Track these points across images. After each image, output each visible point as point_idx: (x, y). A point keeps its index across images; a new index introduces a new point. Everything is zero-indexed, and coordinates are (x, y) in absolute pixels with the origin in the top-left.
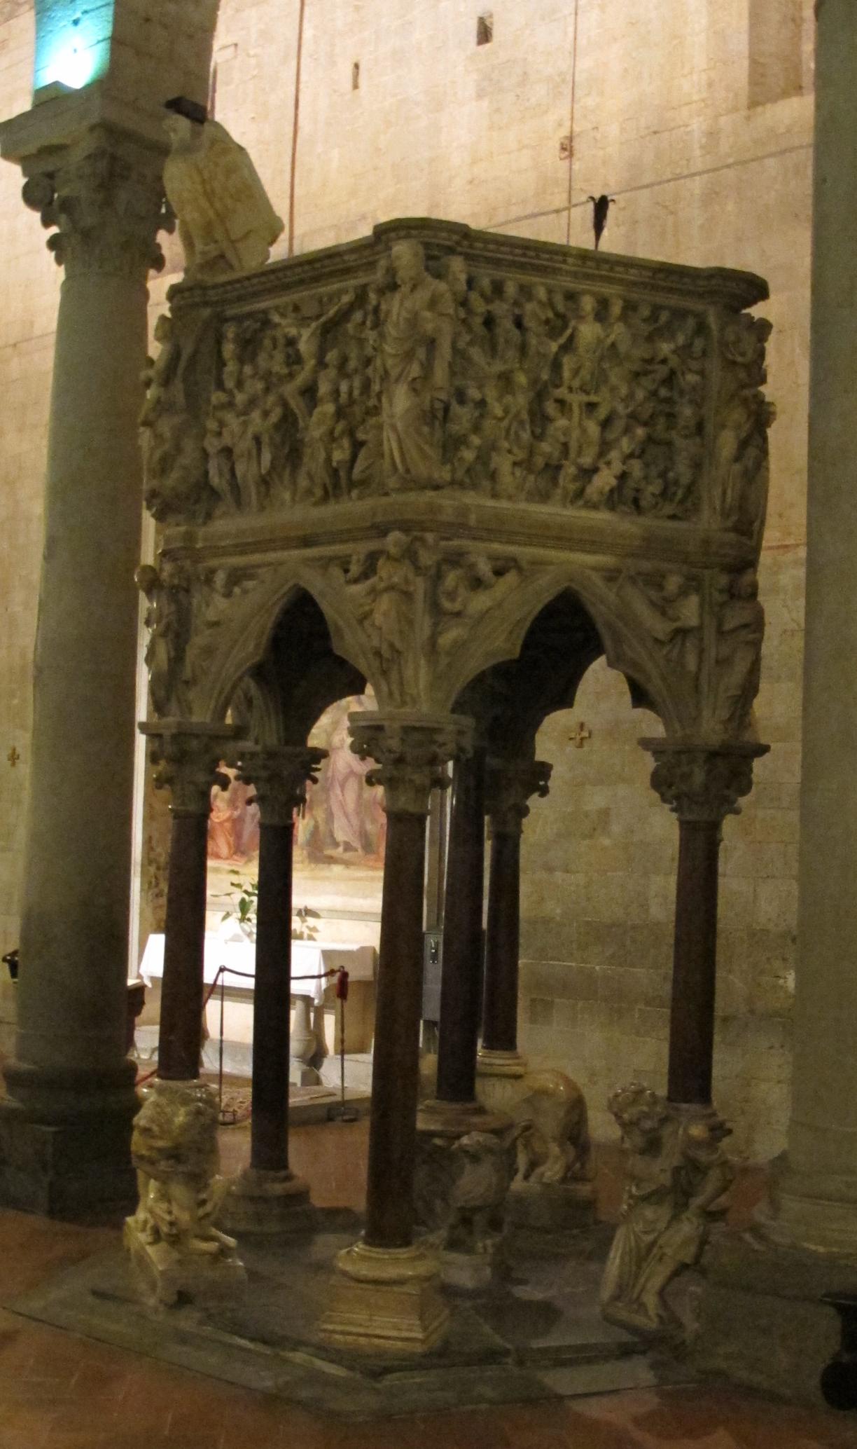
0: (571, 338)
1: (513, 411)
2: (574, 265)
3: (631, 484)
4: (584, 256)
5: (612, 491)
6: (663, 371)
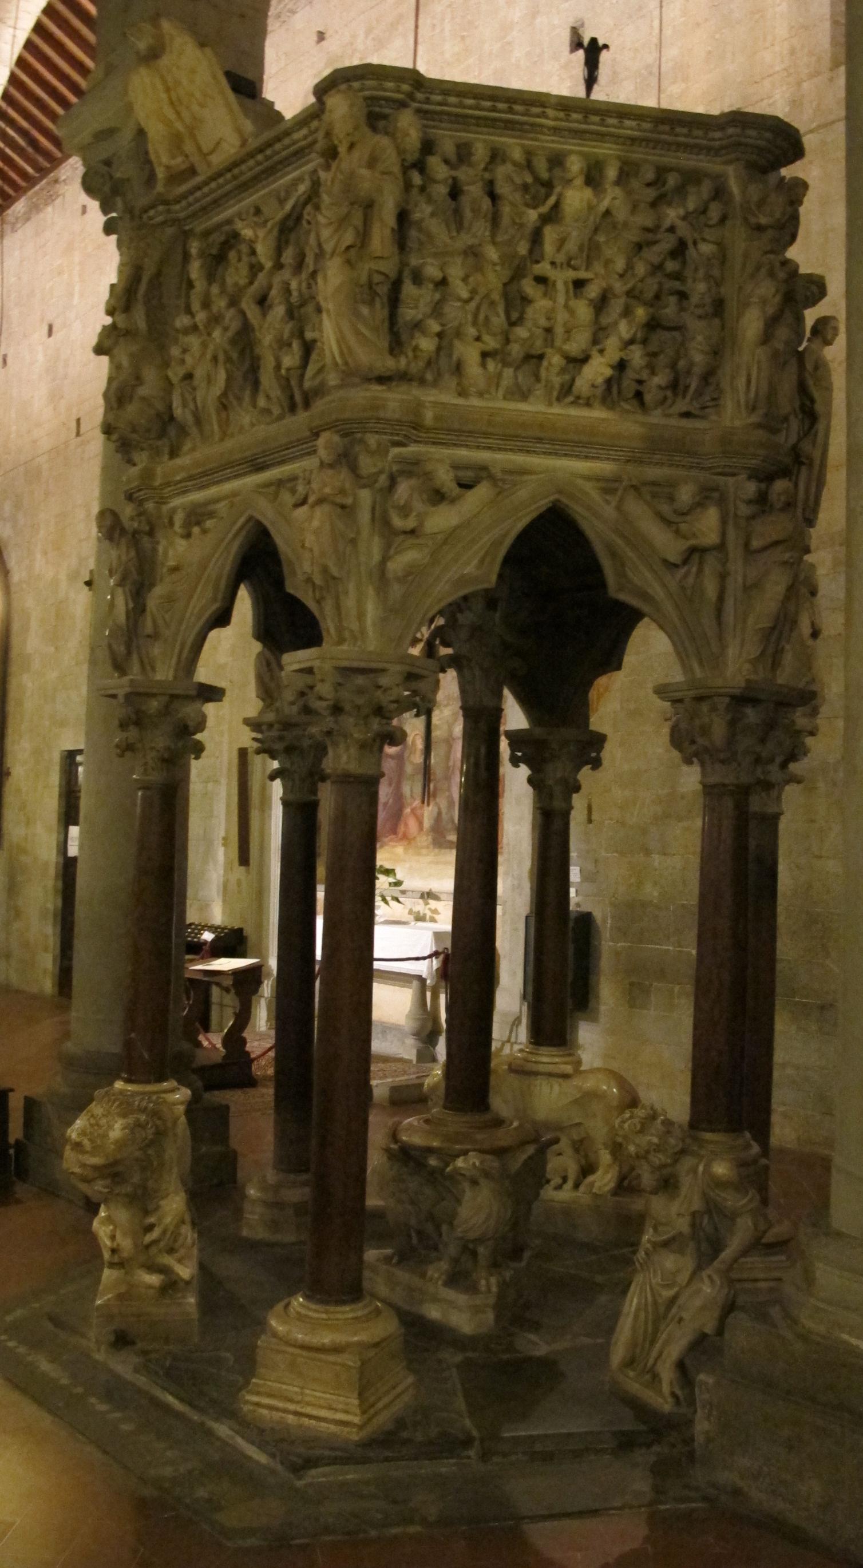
0: (556, 206)
1: (482, 291)
2: (556, 119)
3: (630, 374)
4: (565, 105)
5: (609, 382)
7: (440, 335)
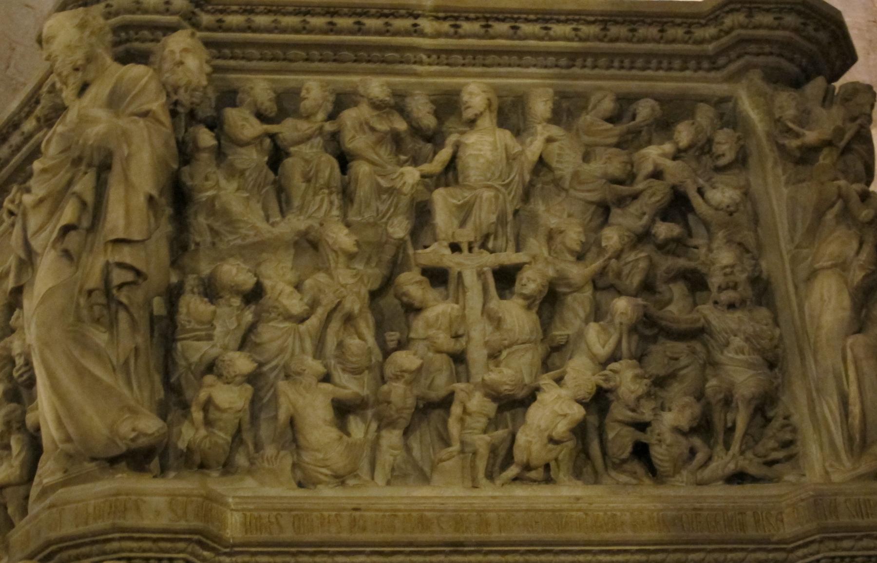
1: (328, 301)
2: (438, 35)
3: (618, 412)
5: (580, 430)
6: (655, 195)
7: (253, 378)
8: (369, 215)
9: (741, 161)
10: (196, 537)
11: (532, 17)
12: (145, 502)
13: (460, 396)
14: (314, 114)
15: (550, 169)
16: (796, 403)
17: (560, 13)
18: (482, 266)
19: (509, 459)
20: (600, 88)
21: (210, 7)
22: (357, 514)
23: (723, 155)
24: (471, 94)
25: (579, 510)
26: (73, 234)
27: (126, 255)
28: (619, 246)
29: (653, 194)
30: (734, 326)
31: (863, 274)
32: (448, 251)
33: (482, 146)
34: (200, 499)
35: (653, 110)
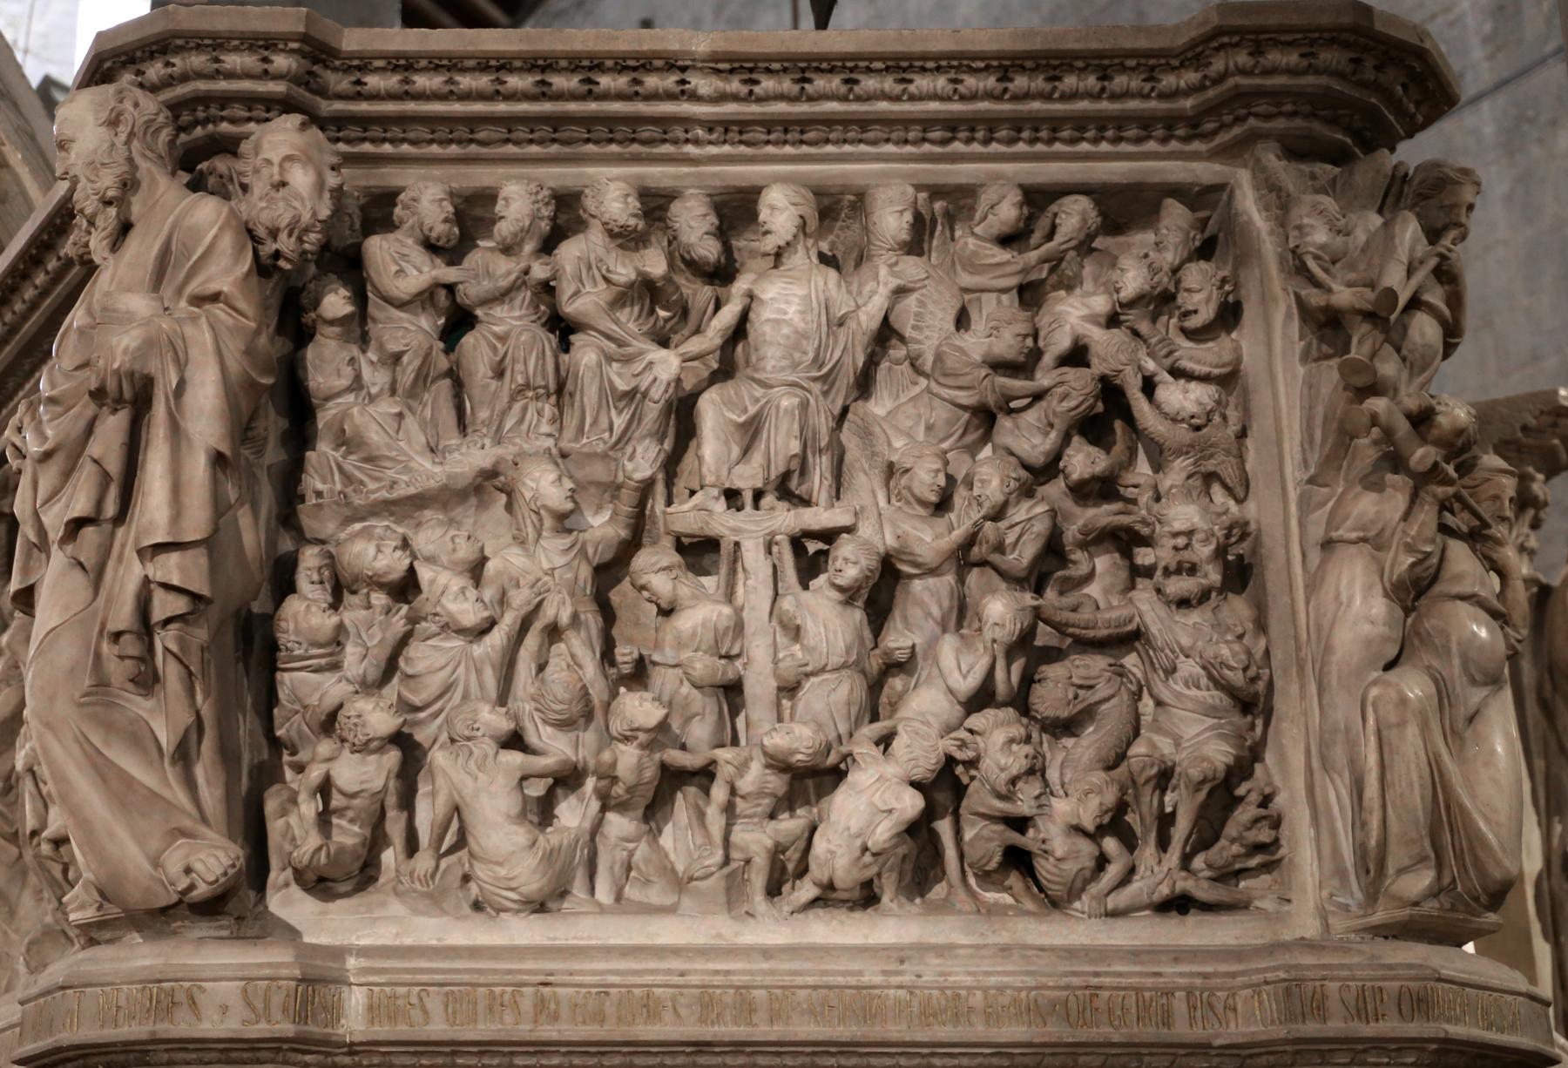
0: (739, 331)
1: (520, 599)
2: (722, 98)
3: (979, 798)
5: (919, 831)
6: (1074, 391)
7: (401, 740)
8: (594, 441)
9: (1229, 315)
10: (285, 1046)
11: (879, 65)
12: (204, 991)
13: (725, 771)
14: (520, 244)
15: (902, 339)
16: (1287, 768)
17: (925, 57)
18: (773, 534)
19: (802, 870)
20: (996, 177)
21: (337, 63)
22: (546, 990)
23: (1196, 312)
24: (773, 208)
25: (900, 987)
26: (89, 532)
27: (170, 568)
28: (1000, 498)
29: (1064, 397)
30: (1186, 641)
31: (1411, 560)
32: (721, 505)
33: (787, 301)
34: (293, 983)
35: (1084, 220)
